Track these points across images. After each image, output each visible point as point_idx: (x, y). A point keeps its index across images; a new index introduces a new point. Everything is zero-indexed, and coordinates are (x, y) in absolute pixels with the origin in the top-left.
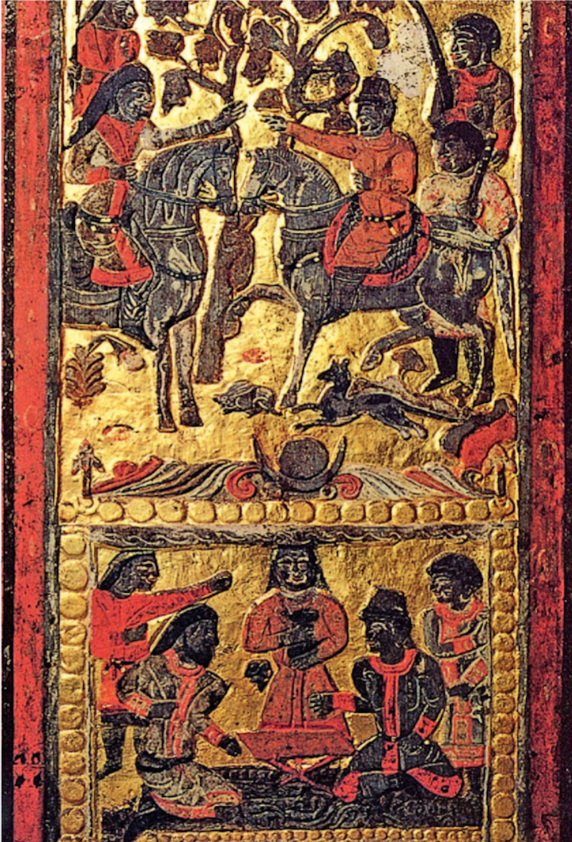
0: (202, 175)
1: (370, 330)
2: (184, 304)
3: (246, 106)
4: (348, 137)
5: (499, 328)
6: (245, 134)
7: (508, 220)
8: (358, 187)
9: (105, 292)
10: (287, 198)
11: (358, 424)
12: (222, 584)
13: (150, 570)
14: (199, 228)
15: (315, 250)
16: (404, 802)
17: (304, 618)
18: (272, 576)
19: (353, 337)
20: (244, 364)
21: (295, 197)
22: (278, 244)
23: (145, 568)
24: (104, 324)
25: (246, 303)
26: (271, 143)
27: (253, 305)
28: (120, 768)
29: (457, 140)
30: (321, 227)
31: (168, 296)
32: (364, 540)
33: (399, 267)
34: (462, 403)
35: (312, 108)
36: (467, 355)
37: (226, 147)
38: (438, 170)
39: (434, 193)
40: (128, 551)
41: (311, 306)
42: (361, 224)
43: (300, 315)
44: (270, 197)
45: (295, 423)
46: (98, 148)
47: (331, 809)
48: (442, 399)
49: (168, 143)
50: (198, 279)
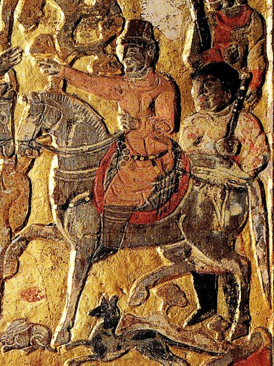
1: (137, 268)
3: (22, 52)
4: (115, 78)
5: (255, 263)
6: (22, 79)
7: (261, 158)
8: (124, 127)
10: (60, 139)
11: (126, 360)
15: (86, 189)
19: (120, 274)
20: (23, 302)
21: (67, 138)
22: (52, 185)
25: (24, 243)
26: (46, 87)
27: (30, 245)
29: (214, 80)
30: (91, 167)
33: (162, 205)
34: (222, 336)
35: (82, 52)
36: (225, 290)
38: (198, 109)
39: (194, 132)
41: (82, 245)
42: (128, 164)
43: (73, 254)
44: (44, 140)
45: (69, 360)
48: (203, 334)
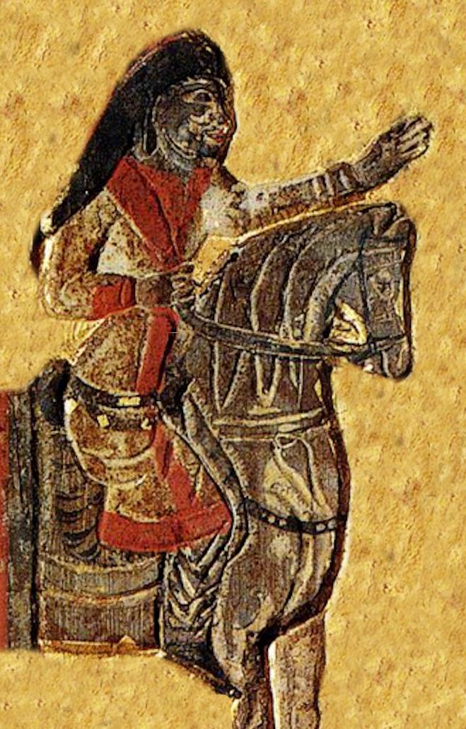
0: (336, 291)
2: (300, 590)
9: (130, 567)
14: (329, 412)
24: (126, 639)
31: (260, 569)
37: (387, 225)
46: (112, 235)
49: (262, 219)
50: (327, 530)
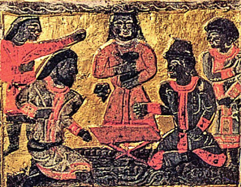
12: (80, 37)
13: (36, 28)
16: (191, 169)
17: (130, 57)
18: (110, 32)
23: (33, 27)
28: (18, 149)
32: (166, 10)
40: (23, 17)
47: (146, 174)
